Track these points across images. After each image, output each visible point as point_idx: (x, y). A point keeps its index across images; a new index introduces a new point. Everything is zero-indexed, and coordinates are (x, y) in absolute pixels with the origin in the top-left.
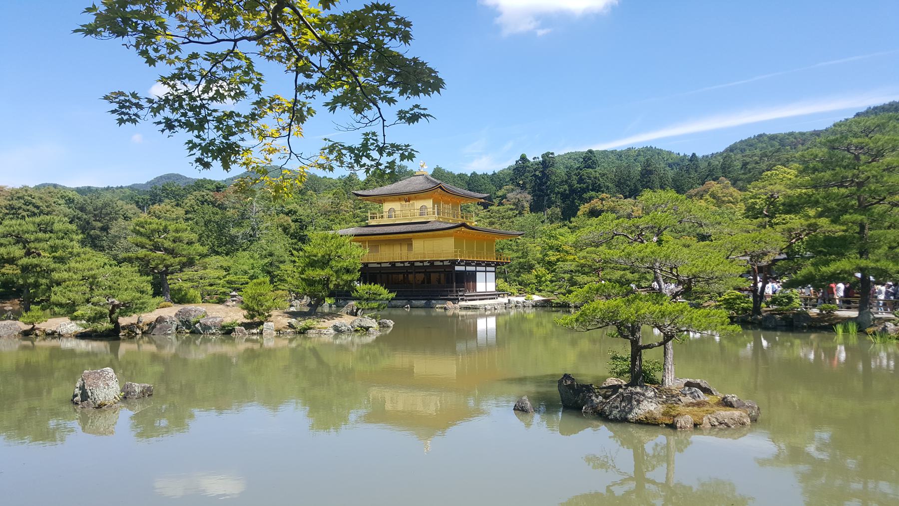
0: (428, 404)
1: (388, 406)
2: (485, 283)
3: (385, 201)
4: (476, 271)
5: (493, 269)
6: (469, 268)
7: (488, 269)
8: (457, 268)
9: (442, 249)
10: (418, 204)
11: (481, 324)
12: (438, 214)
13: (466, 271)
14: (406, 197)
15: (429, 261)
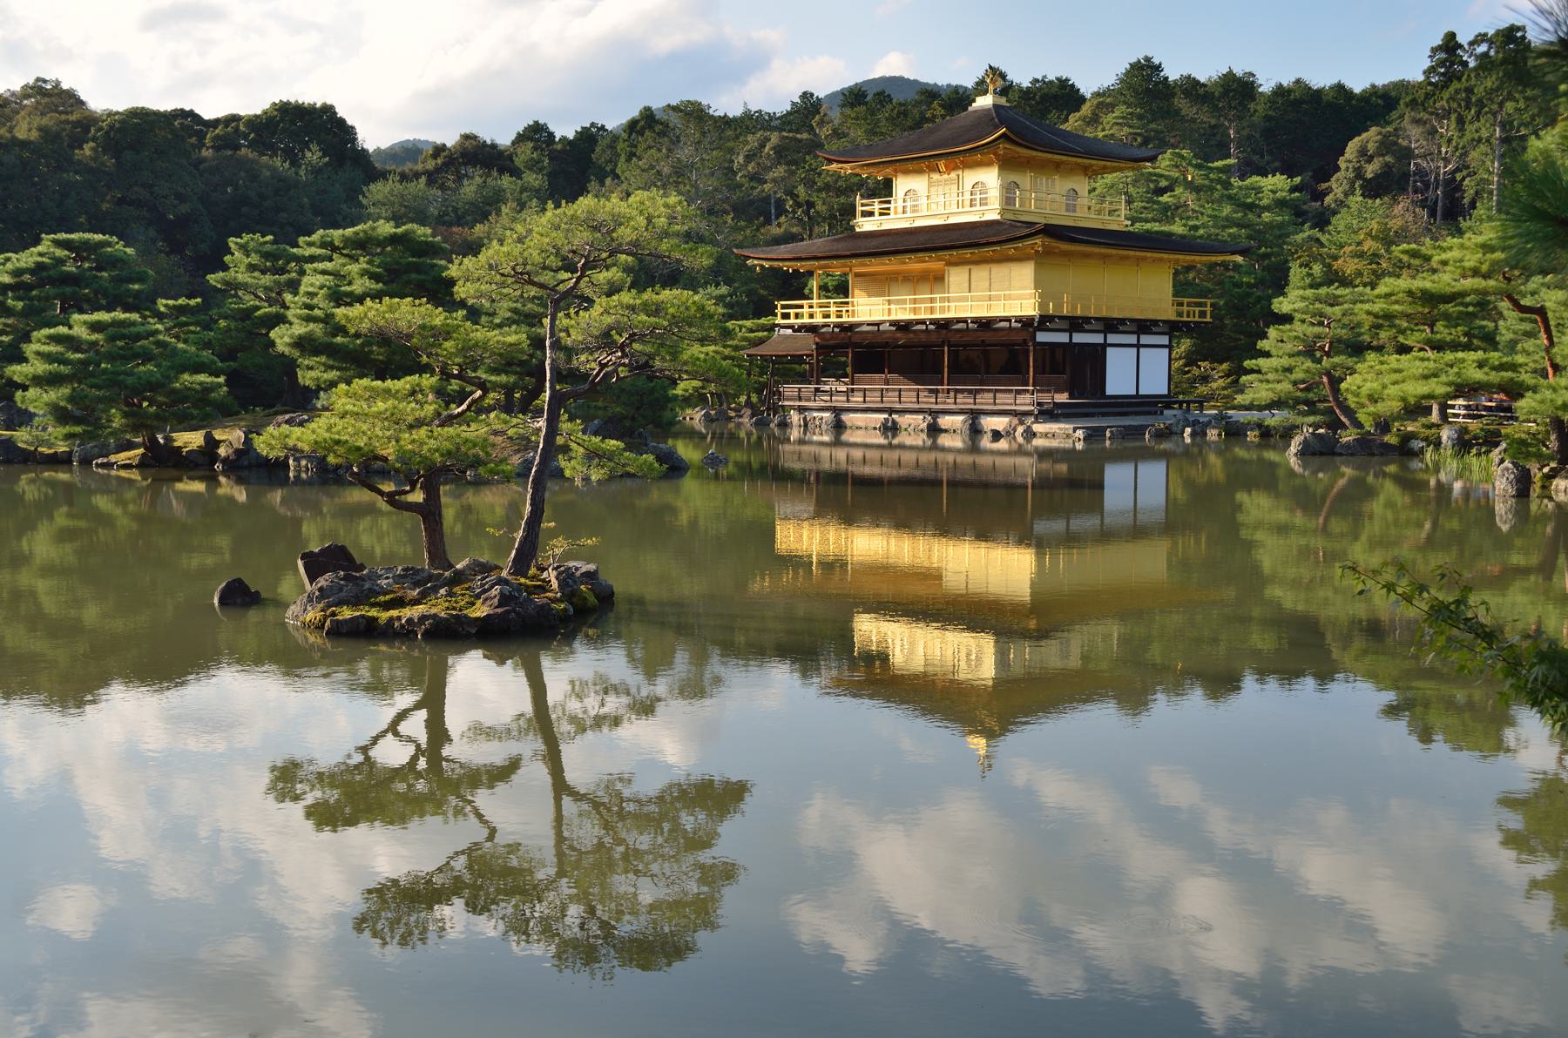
0: (971, 656)
1: (898, 658)
2: (1135, 370)
3: (896, 171)
4: (1105, 345)
5: (1165, 340)
6: (1079, 338)
7: (1145, 339)
8: (1041, 337)
9: (1006, 294)
10: (971, 177)
11: (1117, 477)
12: (1008, 200)
13: (1070, 345)
14: (942, 165)
15: (976, 320)
